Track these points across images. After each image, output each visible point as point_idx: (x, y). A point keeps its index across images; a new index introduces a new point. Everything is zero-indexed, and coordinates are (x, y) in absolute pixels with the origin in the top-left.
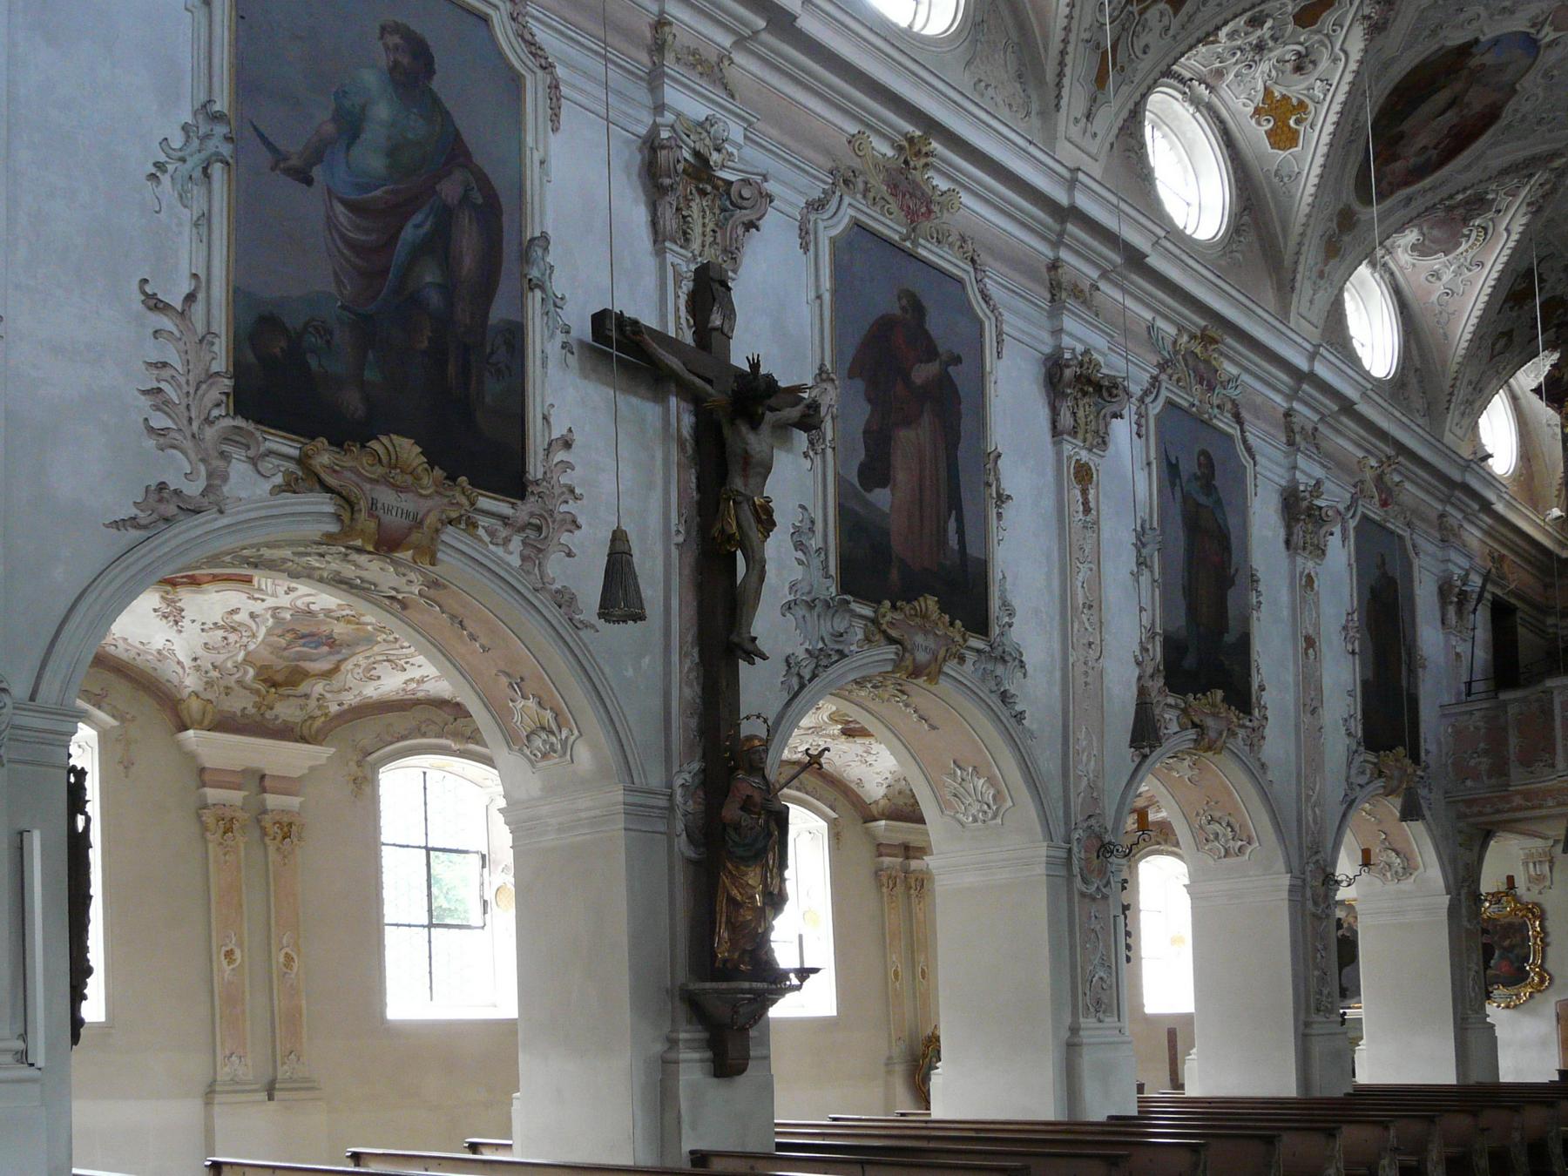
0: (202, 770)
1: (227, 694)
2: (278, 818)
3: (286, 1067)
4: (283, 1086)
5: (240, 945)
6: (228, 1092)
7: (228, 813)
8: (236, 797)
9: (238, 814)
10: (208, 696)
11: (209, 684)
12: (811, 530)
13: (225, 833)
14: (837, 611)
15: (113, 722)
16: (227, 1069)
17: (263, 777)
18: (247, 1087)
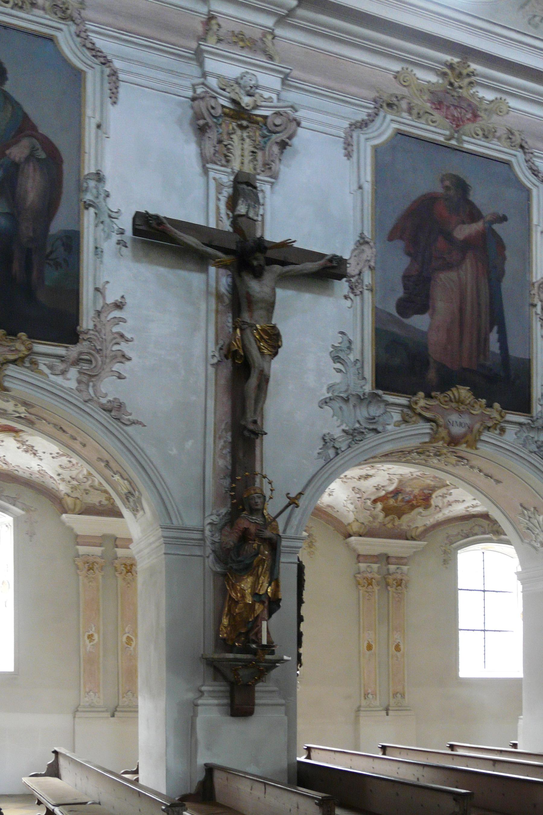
0: (77, 536)
1: (87, 493)
2: (124, 562)
3: (125, 699)
4: (121, 709)
5: (98, 632)
6: (84, 712)
7: (91, 559)
8: (97, 550)
9: (99, 560)
10: (75, 495)
11: (74, 488)
12: (349, 348)
13: (89, 570)
14: (370, 402)
15: (23, 512)
16: (87, 699)
17: (116, 539)
18: (97, 709)
